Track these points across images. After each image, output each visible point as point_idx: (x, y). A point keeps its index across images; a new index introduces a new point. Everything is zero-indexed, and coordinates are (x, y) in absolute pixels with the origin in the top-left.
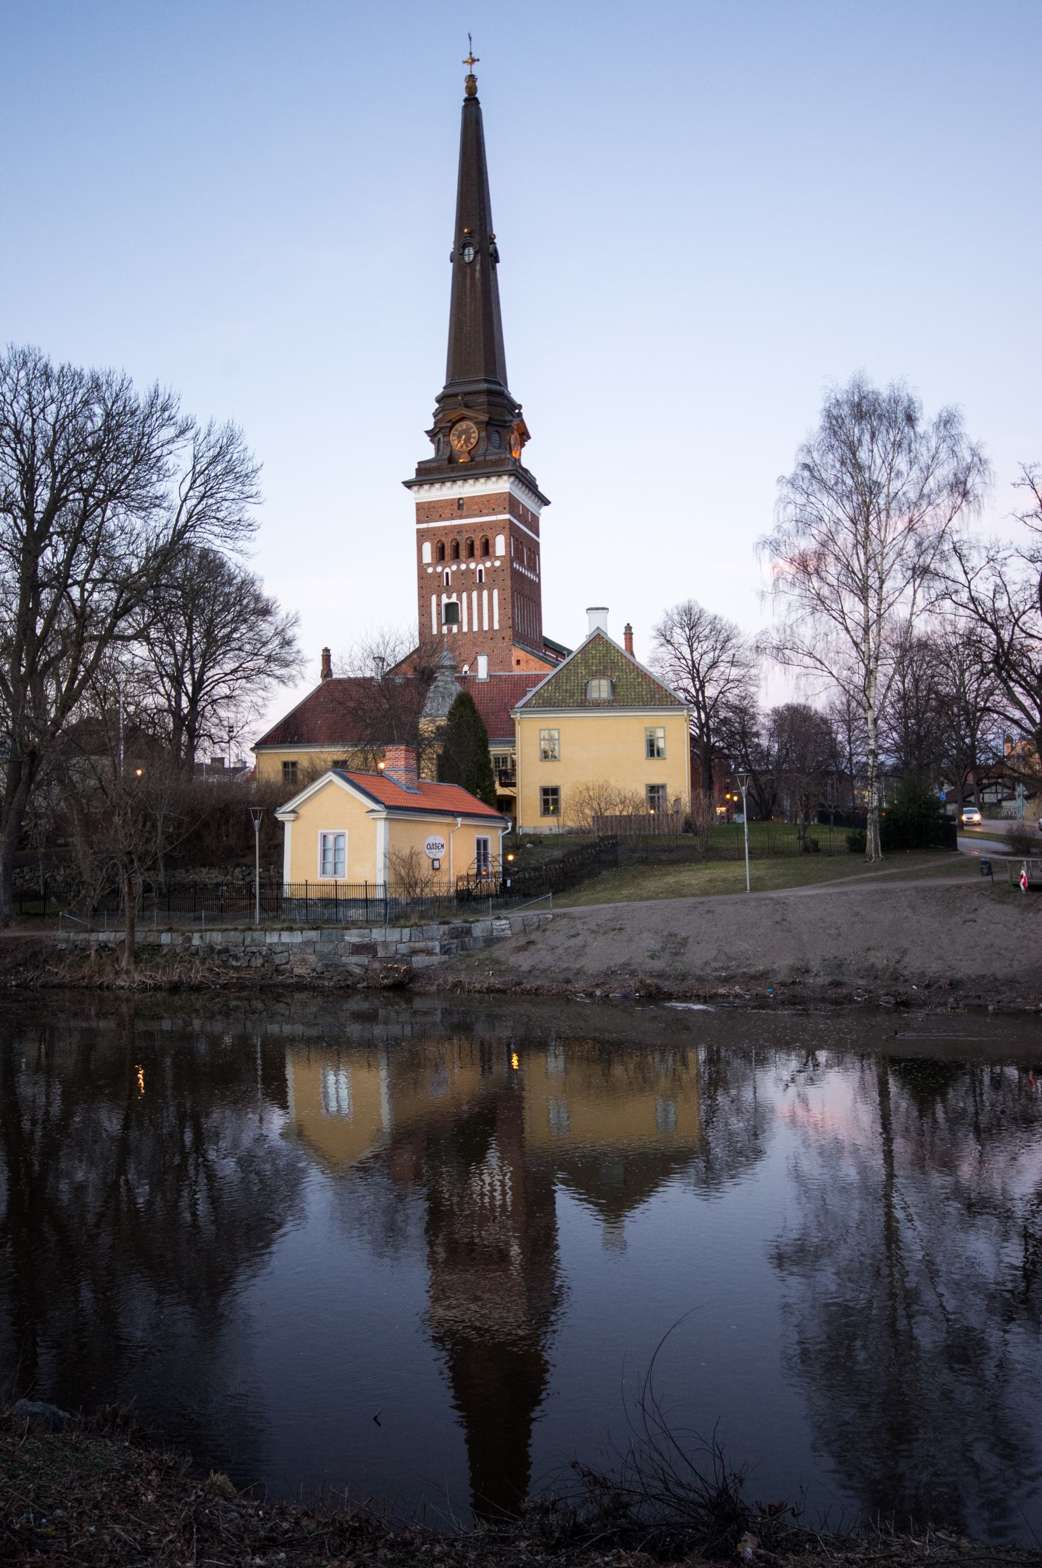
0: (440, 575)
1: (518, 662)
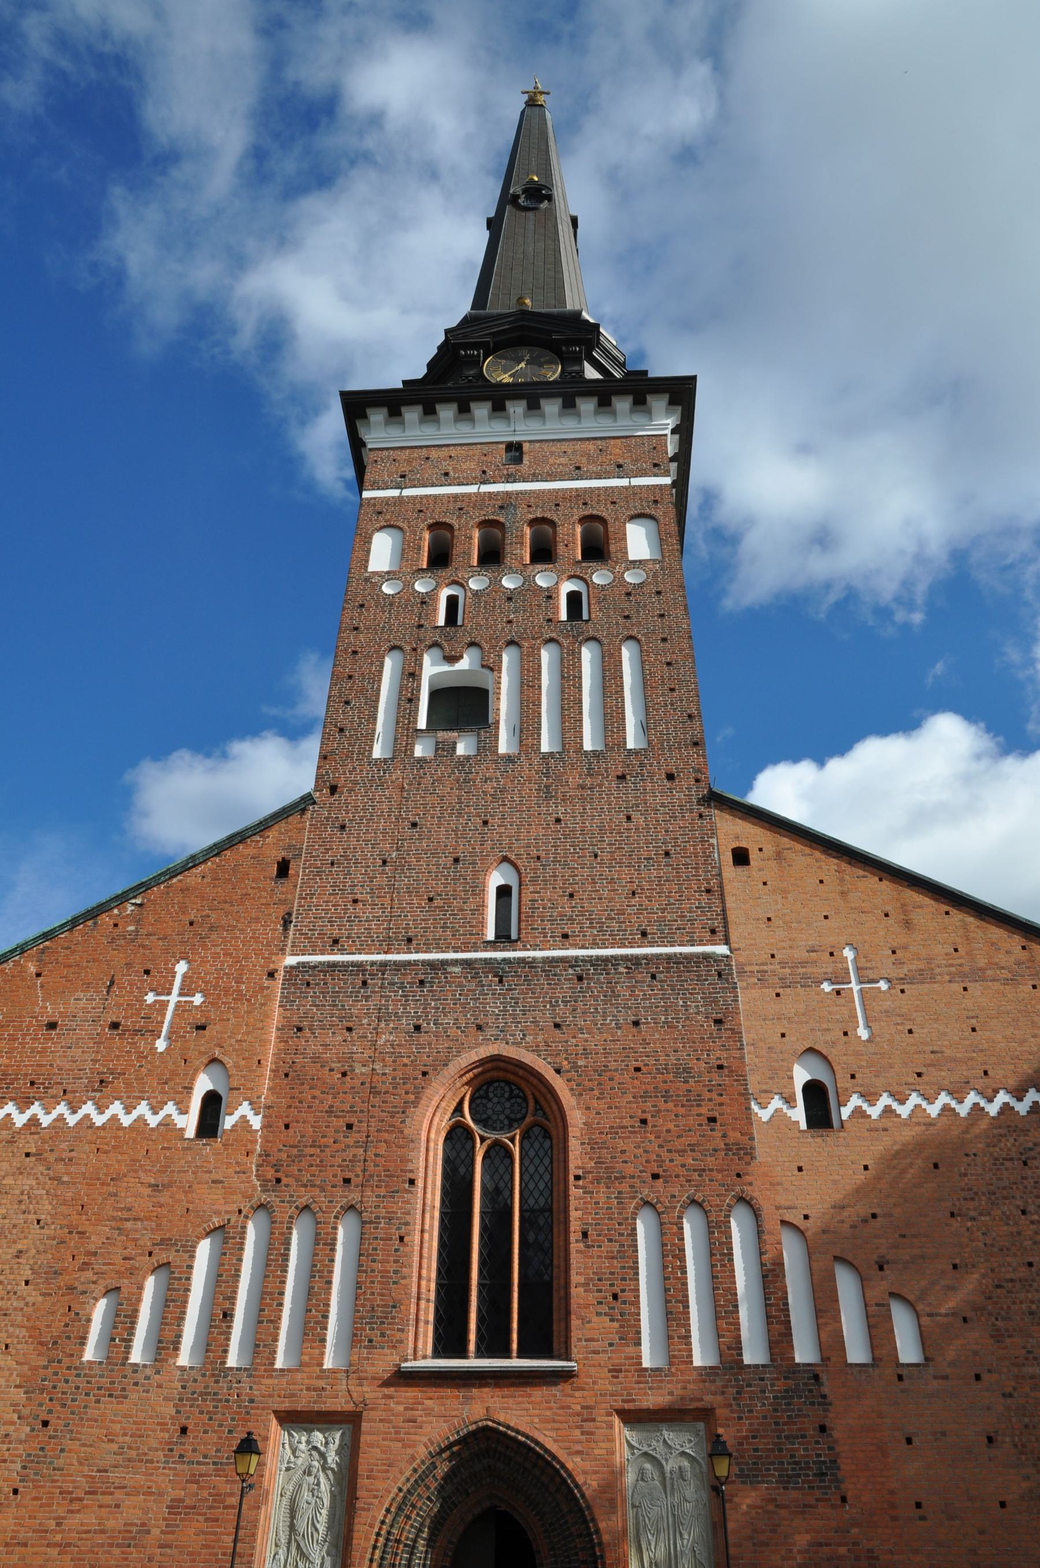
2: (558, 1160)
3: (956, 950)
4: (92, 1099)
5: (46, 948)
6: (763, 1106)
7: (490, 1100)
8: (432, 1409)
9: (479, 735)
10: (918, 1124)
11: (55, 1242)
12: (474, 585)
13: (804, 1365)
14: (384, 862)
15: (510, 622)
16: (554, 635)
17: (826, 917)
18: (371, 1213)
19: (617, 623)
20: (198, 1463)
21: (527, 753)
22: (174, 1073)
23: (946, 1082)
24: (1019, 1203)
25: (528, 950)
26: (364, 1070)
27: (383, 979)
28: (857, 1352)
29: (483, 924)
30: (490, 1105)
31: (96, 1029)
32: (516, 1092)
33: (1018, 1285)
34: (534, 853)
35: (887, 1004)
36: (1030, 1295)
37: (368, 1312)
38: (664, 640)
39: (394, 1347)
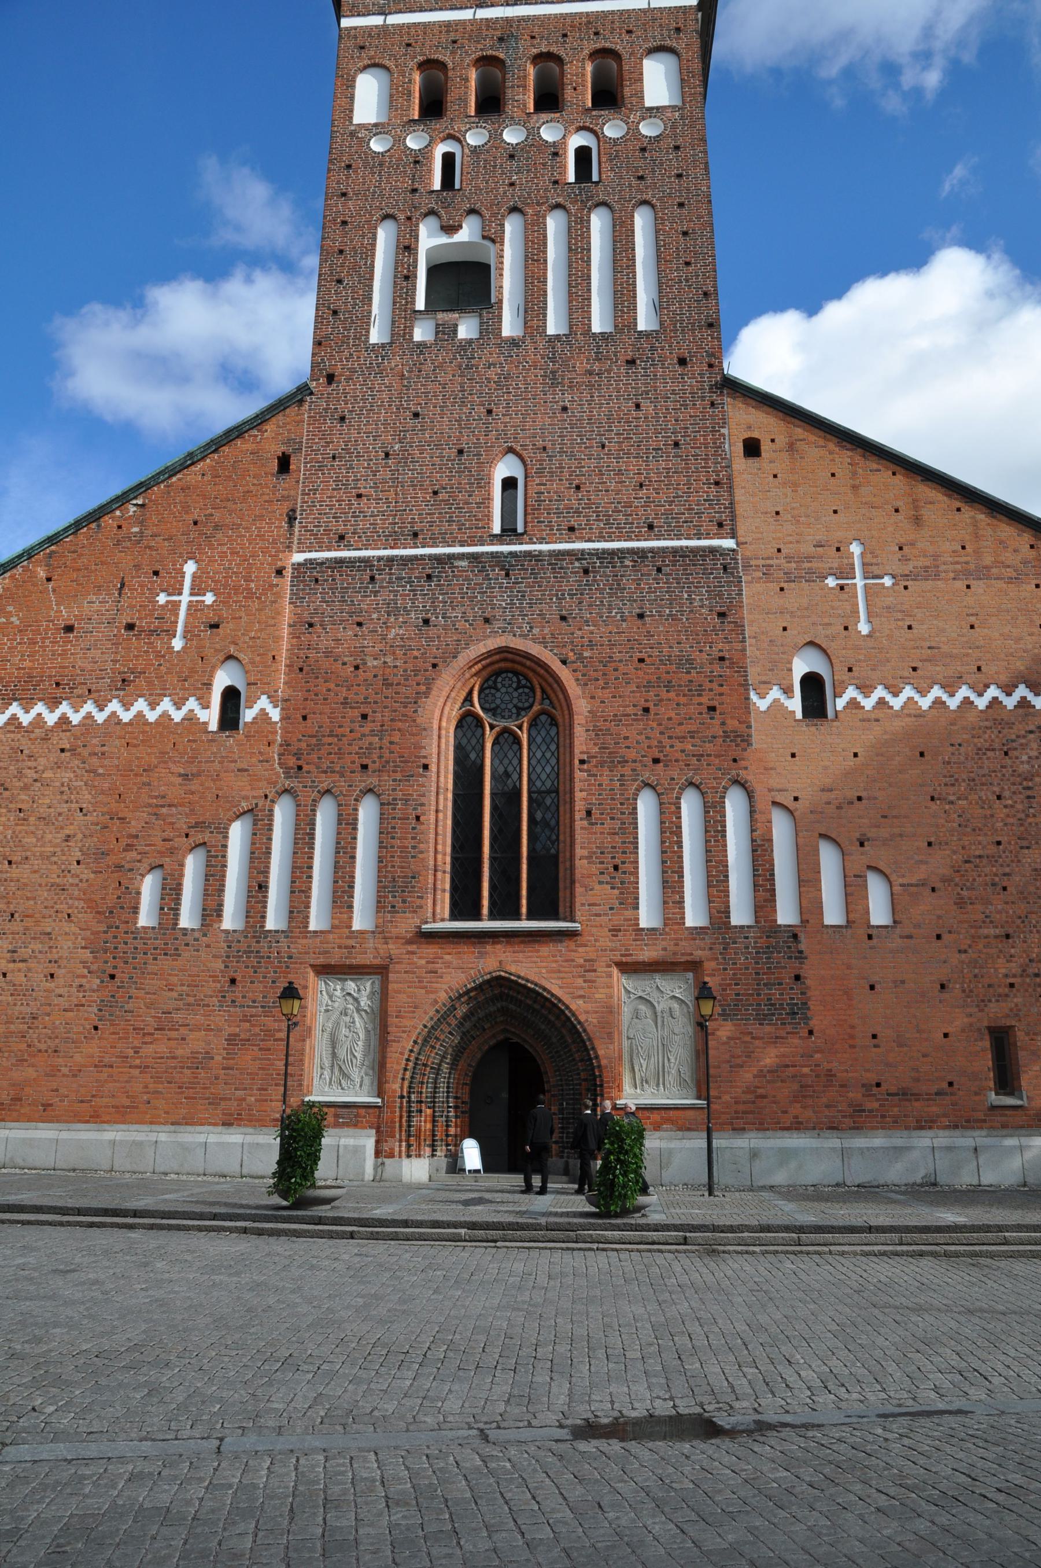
0: (420, 160)
1: (752, 448)
2: (564, 746)
3: (963, 548)
4: (117, 697)
5: (53, 552)
6: (762, 697)
7: (498, 690)
8: (451, 963)
9: (481, 315)
10: (909, 715)
11: (98, 827)
12: (473, 139)
13: (785, 926)
14: (387, 455)
15: (512, 184)
16: (560, 200)
17: (835, 512)
18: (389, 795)
19: (630, 185)
20: (248, 1007)
21: (532, 337)
22: (193, 671)
23: (940, 677)
24: (996, 789)
25: (535, 543)
26: (375, 663)
27: (391, 574)
28: (833, 915)
29: (489, 517)
30: (498, 695)
31: (112, 631)
32: (524, 682)
33: (985, 861)
34: (540, 443)
35: (889, 600)
36: (994, 869)
37: (389, 882)
38: (681, 205)
39: (415, 912)
